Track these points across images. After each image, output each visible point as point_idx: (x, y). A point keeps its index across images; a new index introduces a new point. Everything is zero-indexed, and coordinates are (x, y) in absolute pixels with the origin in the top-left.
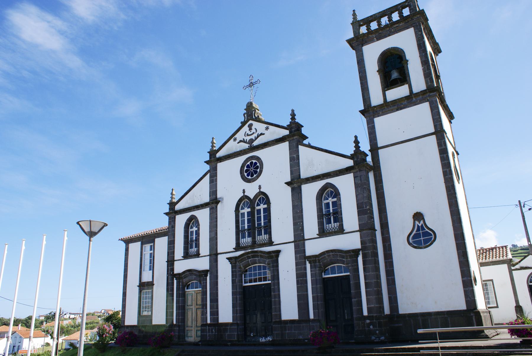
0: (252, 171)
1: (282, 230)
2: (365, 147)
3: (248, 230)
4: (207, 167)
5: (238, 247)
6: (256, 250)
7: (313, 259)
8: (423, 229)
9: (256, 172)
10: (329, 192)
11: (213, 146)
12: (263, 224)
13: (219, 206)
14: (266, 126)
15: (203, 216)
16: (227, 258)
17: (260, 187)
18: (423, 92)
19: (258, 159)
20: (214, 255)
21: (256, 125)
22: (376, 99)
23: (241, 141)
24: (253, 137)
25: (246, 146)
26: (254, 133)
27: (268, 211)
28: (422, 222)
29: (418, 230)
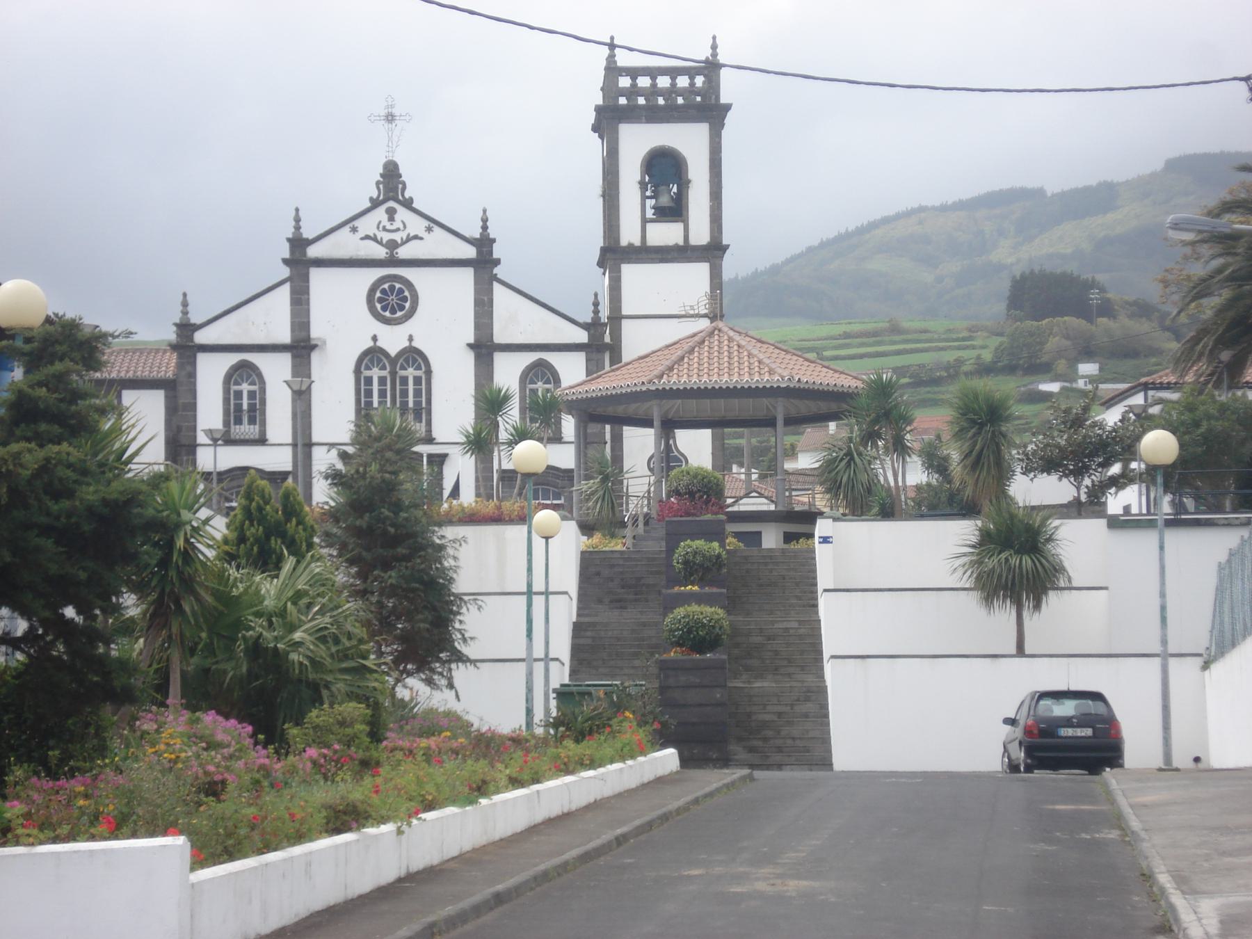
0: (393, 301)
2: (604, 314)
4: (285, 272)
13: (315, 357)
15: (276, 370)
17: (411, 339)
19: (409, 285)
20: (303, 444)
21: (402, 214)
23: (367, 237)
24: (397, 237)
25: (381, 253)
26: (398, 230)
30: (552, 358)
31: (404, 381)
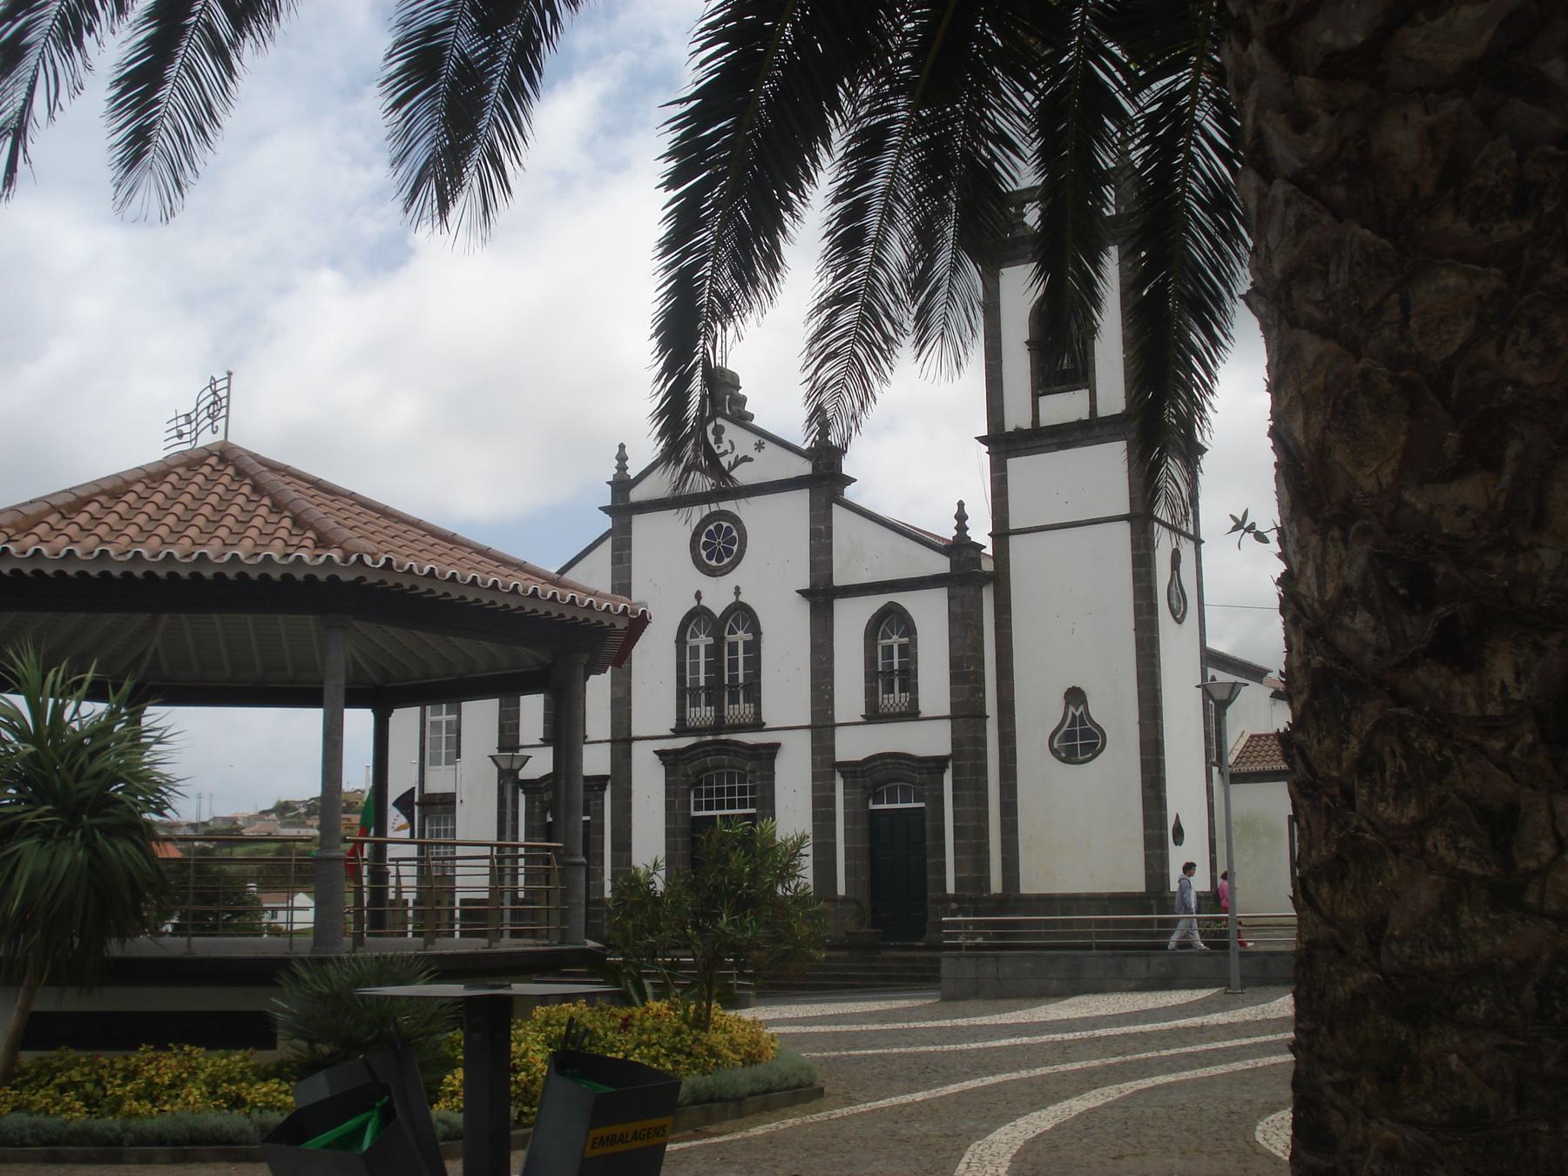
0: (719, 547)
1: (784, 696)
2: (980, 532)
3: (707, 688)
4: (606, 523)
5: (681, 730)
6: (723, 737)
7: (852, 770)
8: (1082, 723)
9: (729, 552)
10: (891, 621)
11: (622, 467)
12: (741, 680)
14: (756, 439)
16: (658, 753)
17: (737, 591)
18: (1114, 419)
19: (735, 520)
20: (622, 742)
22: (1017, 416)
27: (754, 648)
28: (1081, 708)
29: (1073, 724)
30: (904, 599)
31: (733, 647)
